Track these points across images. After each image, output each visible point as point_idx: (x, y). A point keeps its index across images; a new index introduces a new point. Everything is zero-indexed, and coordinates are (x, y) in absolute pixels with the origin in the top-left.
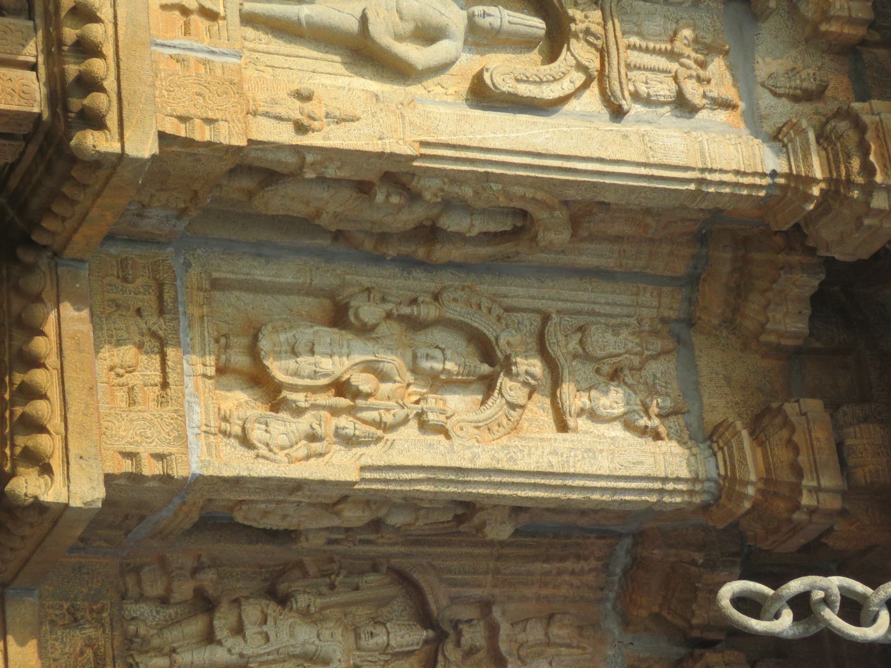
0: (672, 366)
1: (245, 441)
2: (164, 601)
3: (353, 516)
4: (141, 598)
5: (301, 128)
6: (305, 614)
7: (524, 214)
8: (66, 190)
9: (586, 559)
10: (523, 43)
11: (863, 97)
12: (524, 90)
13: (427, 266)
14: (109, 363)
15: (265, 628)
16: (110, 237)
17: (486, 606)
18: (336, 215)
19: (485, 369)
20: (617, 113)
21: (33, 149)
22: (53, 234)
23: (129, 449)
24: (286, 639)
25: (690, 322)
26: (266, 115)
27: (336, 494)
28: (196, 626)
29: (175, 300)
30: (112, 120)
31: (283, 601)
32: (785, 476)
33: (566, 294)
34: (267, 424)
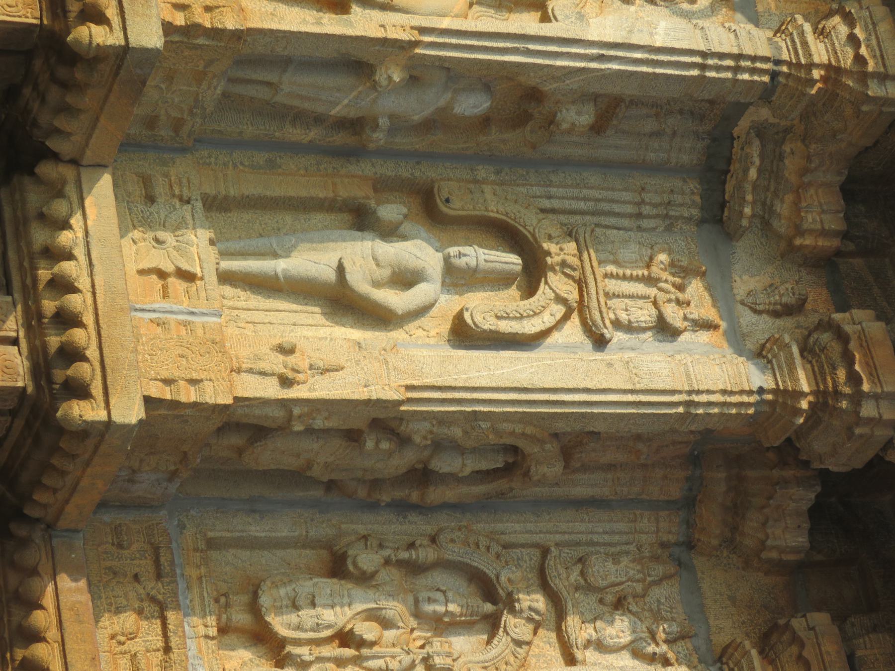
5: (286, 382)
8: (55, 461)
10: (501, 280)
11: (843, 308)
12: (505, 327)
13: (421, 509)
14: (110, 631)
16: (103, 505)
18: (327, 466)
19: (488, 607)
20: (600, 342)
21: (19, 423)
22: (45, 506)
25: (690, 545)
26: (250, 371)
29: (172, 563)
30: (96, 389)
33: (563, 526)
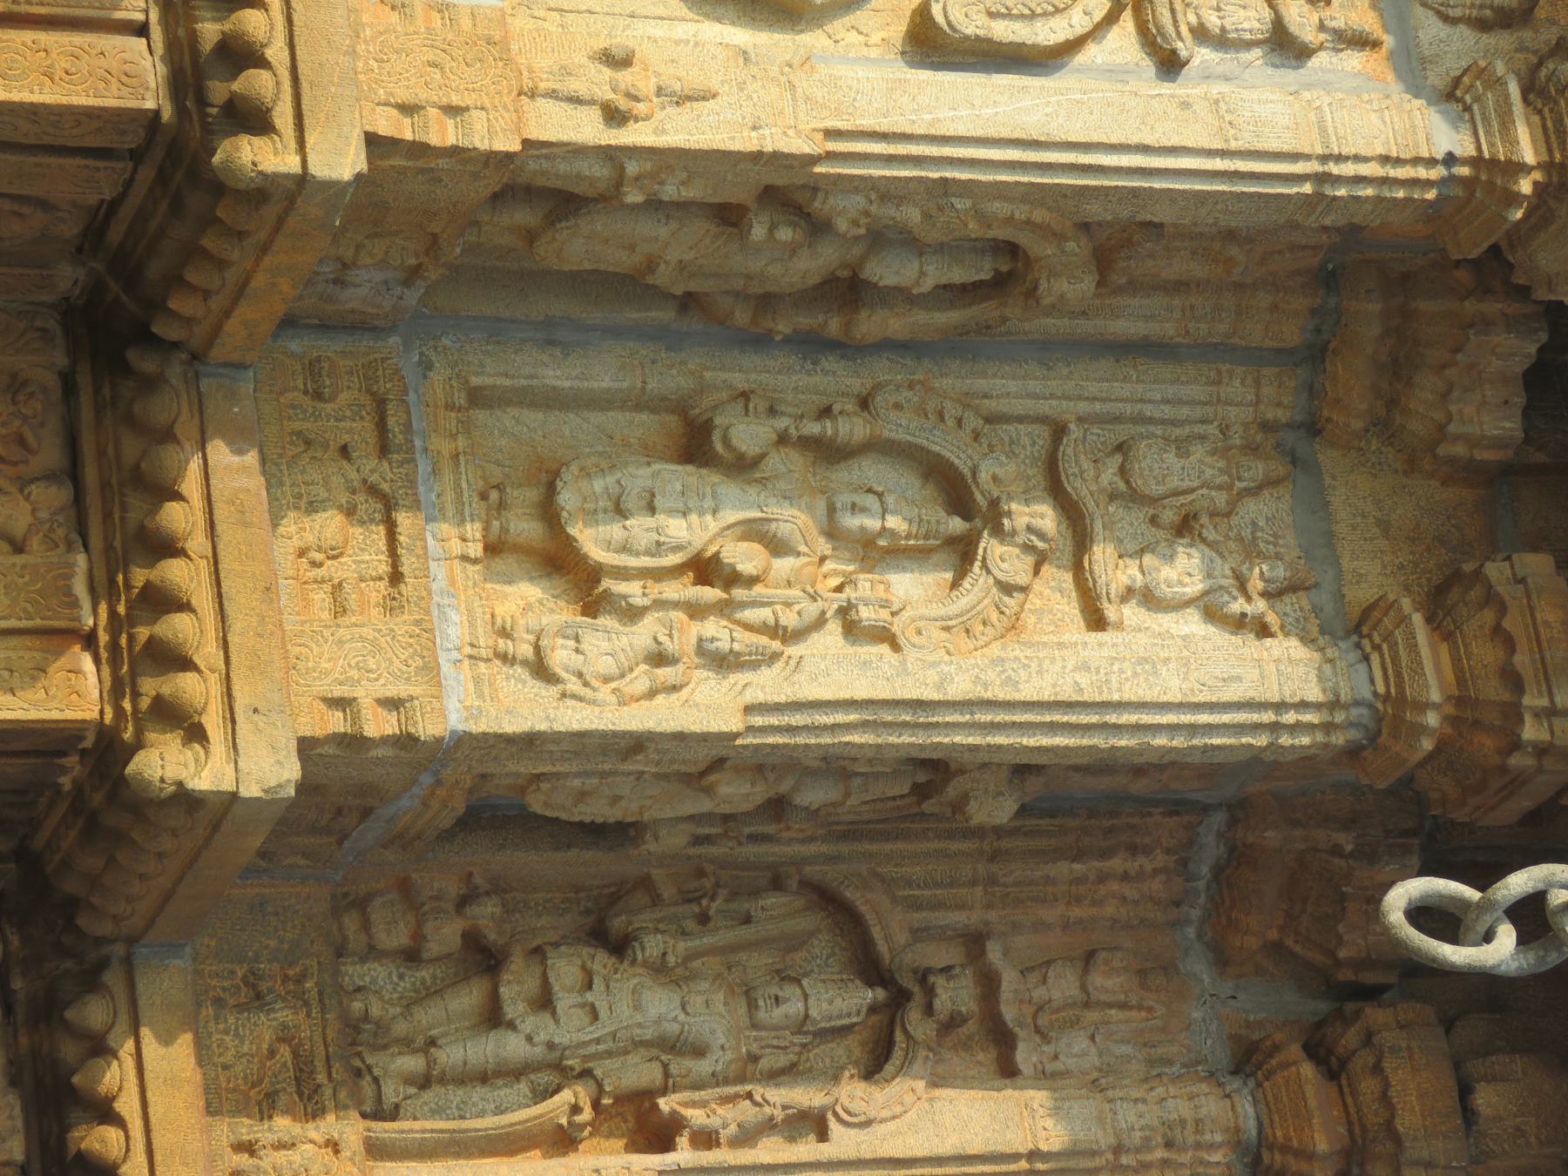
0: (1285, 505)
1: (541, 670)
2: (411, 956)
3: (736, 793)
4: (372, 952)
5: (614, 116)
6: (660, 969)
7: (1012, 249)
8: (208, 243)
9: (1147, 851)
12: (1004, 31)
14: (297, 542)
15: (589, 997)
16: (289, 323)
17: (975, 942)
18: (682, 265)
19: (956, 525)
20: (1170, 65)
21: (147, 174)
22: (189, 321)
23: (337, 692)
24: (627, 1013)
25: (1313, 428)
26: (553, 95)
27: (703, 755)
28: (469, 998)
29: (408, 427)
30: (283, 117)
31: (620, 947)
32: (1492, 690)
33: (1093, 388)
34: (577, 639)
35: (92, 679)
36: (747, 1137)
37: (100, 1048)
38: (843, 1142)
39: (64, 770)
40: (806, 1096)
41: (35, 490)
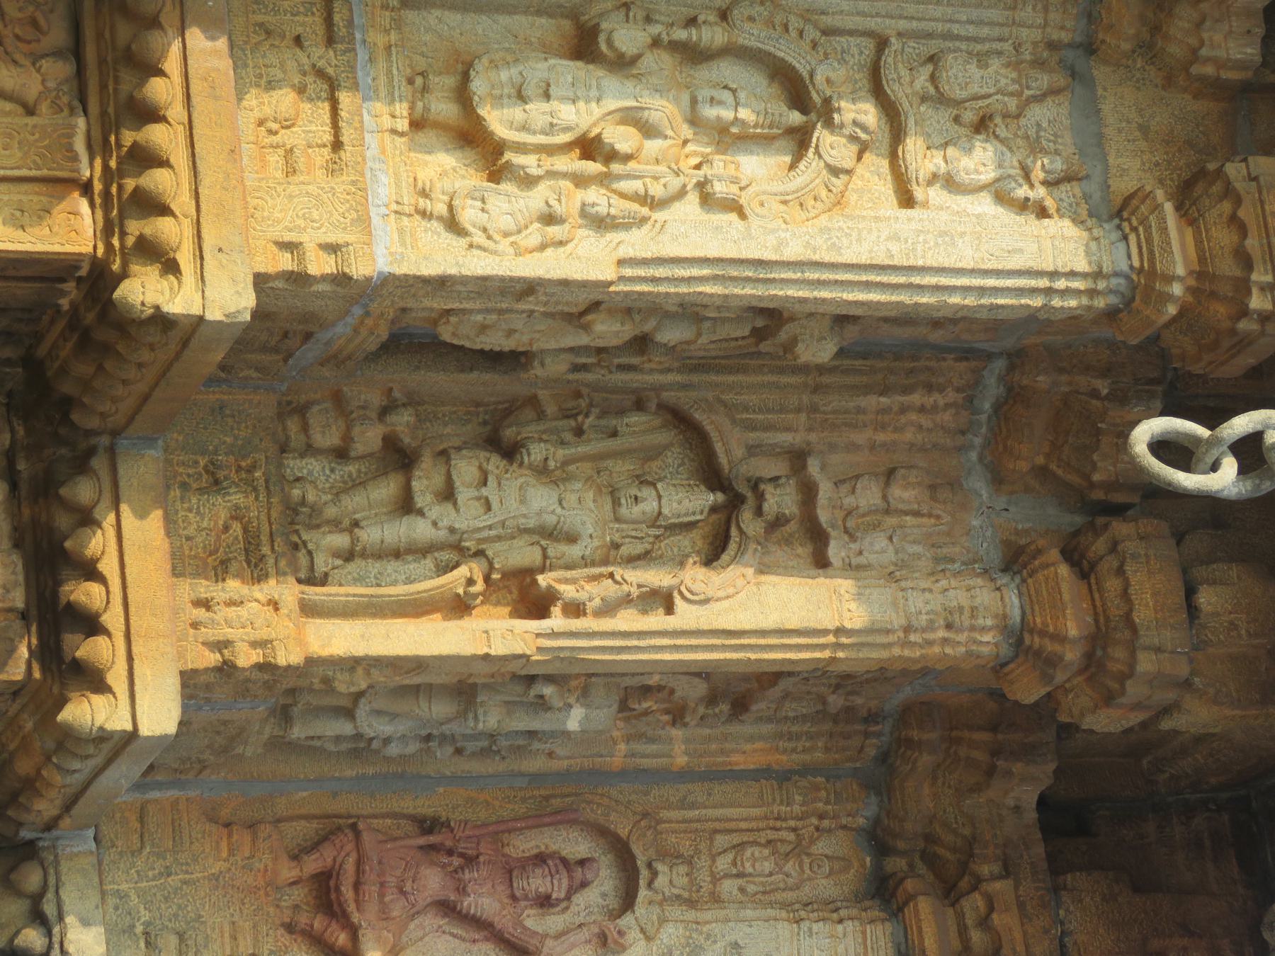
0: (1064, 110)
1: (453, 225)
2: (341, 454)
3: (608, 331)
4: (309, 450)
6: (542, 471)
9: (941, 390)
14: (257, 114)
15: (484, 491)
17: (798, 458)
19: (796, 117)
23: (288, 237)
24: (515, 506)
25: (1090, 48)
27: (583, 298)
28: (386, 490)
29: (350, 23)
31: (510, 452)
32: (1227, 267)
34: (483, 201)
35: (88, 220)
36: (608, 609)
37: (87, 519)
38: (686, 616)
39: (63, 293)
40: (657, 577)
41: (45, 64)
